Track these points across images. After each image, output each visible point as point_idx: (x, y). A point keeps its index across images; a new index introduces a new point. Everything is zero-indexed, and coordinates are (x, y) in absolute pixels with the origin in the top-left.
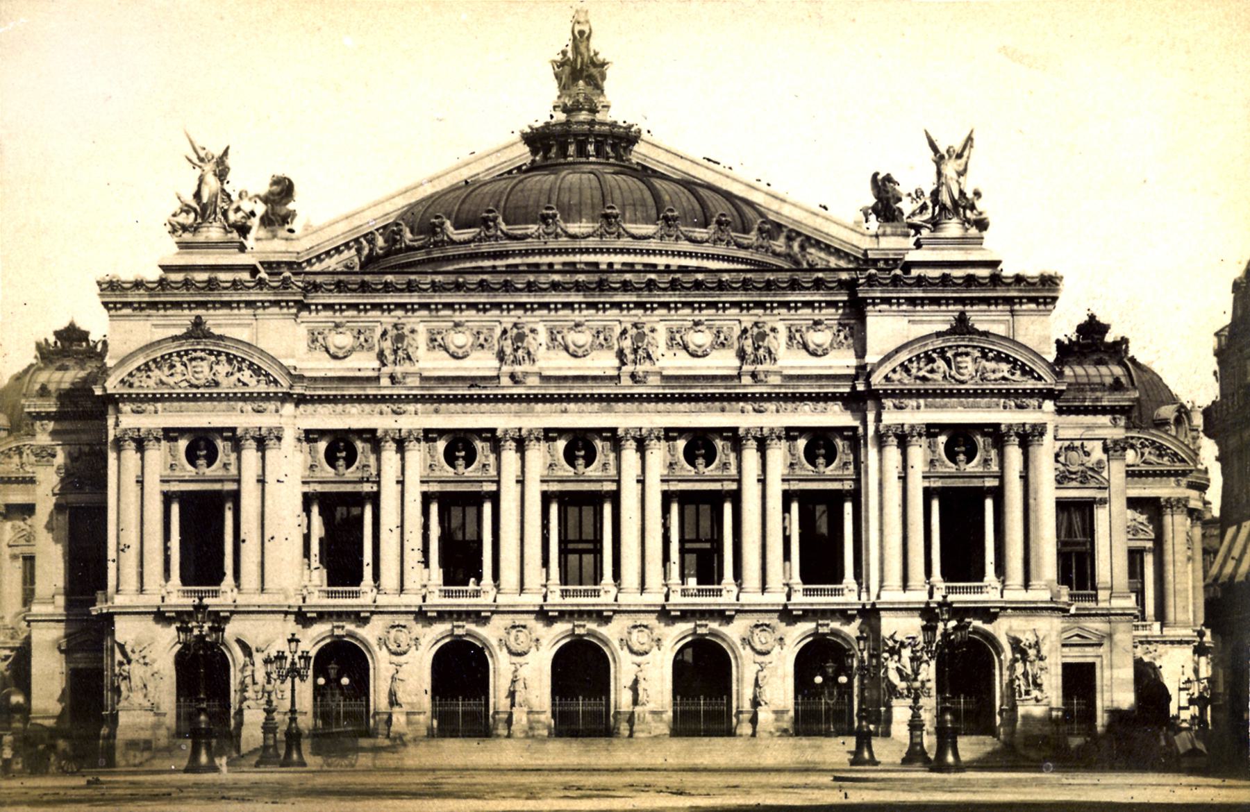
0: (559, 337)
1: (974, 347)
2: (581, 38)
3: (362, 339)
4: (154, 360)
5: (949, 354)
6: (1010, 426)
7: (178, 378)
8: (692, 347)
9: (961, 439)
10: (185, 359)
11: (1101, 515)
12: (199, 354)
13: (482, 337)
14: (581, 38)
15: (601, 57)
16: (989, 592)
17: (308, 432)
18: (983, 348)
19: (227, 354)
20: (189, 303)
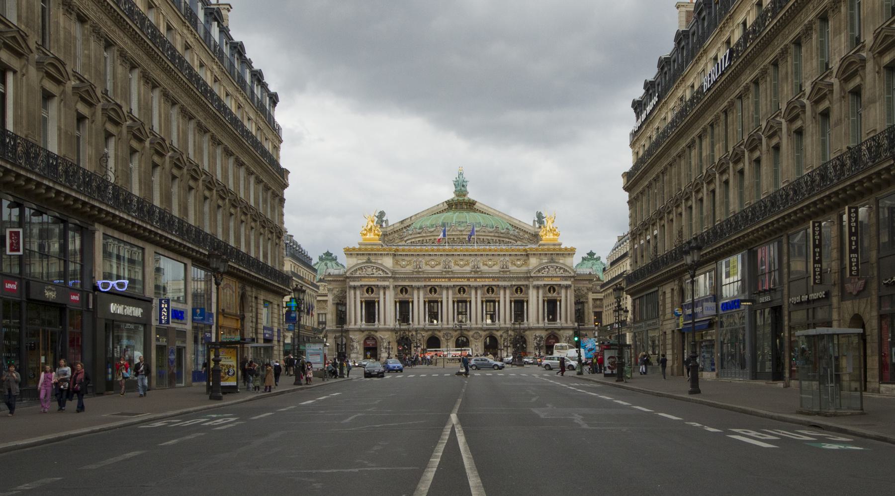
2: (461, 174)
9: (552, 288)
11: (586, 305)
14: (461, 174)
16: (559, 323)
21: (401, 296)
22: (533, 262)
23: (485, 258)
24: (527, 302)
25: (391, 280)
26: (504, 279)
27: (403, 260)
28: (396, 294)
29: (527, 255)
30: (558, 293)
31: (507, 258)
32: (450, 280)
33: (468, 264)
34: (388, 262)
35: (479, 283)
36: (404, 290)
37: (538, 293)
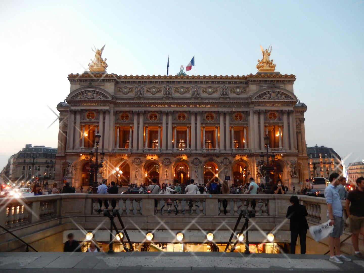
0: (177, 90)
1: (276, 91)
3: (130, 90)
4: (79, 93)
5: (270, 93)
6: (286, 111)
7: (84, 97)
8: (208, 92)
10: (87, 92)
11: (299, 135)
12: (90, 91)
13: (159, 90)
15: (185, 73)
17: (117, 111)
18: (278, 91)
19: (97, 91)
20: (89, 80)
21: (122, 122)
22: (253, 88)
23: (204, 86)
24: (247, 128)
25: (112, 105)
26: (224, 105)
27: (126, 87)
28: (117, 120)
29: (247, 83)
30: (280, 119)
31: (227, 86)
32: (170, 106)
33: (188, 92)
34: (110, 88)
35: (199, 109)
36: (125, 115)
37: (259, 119)
